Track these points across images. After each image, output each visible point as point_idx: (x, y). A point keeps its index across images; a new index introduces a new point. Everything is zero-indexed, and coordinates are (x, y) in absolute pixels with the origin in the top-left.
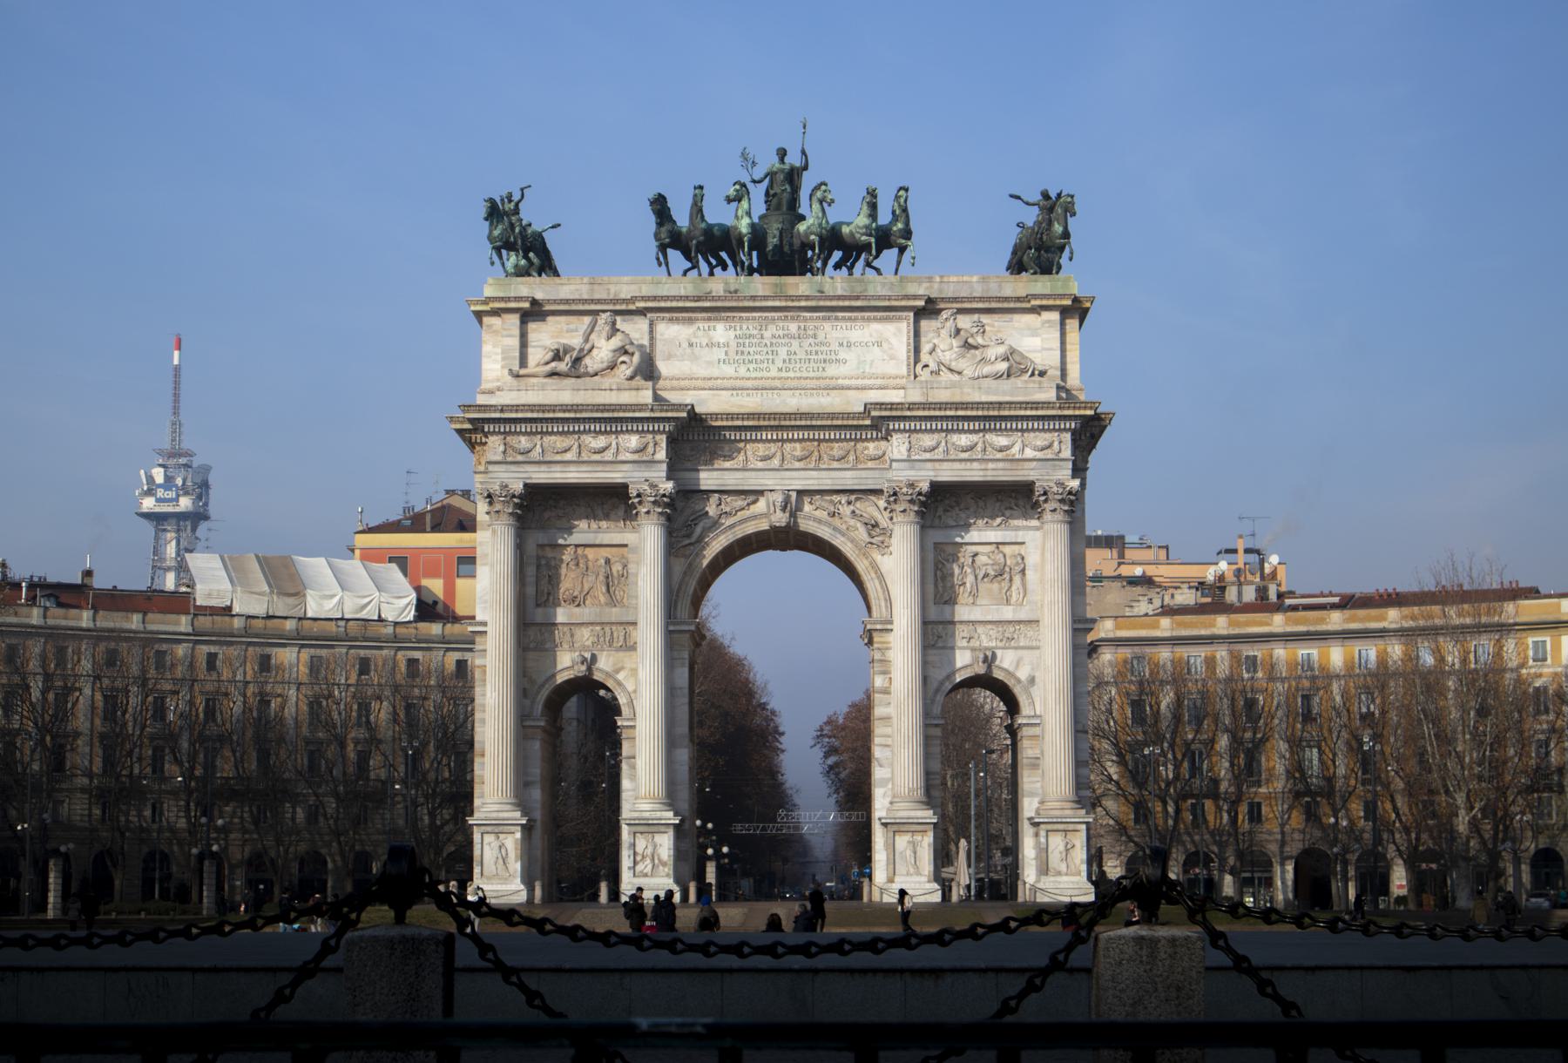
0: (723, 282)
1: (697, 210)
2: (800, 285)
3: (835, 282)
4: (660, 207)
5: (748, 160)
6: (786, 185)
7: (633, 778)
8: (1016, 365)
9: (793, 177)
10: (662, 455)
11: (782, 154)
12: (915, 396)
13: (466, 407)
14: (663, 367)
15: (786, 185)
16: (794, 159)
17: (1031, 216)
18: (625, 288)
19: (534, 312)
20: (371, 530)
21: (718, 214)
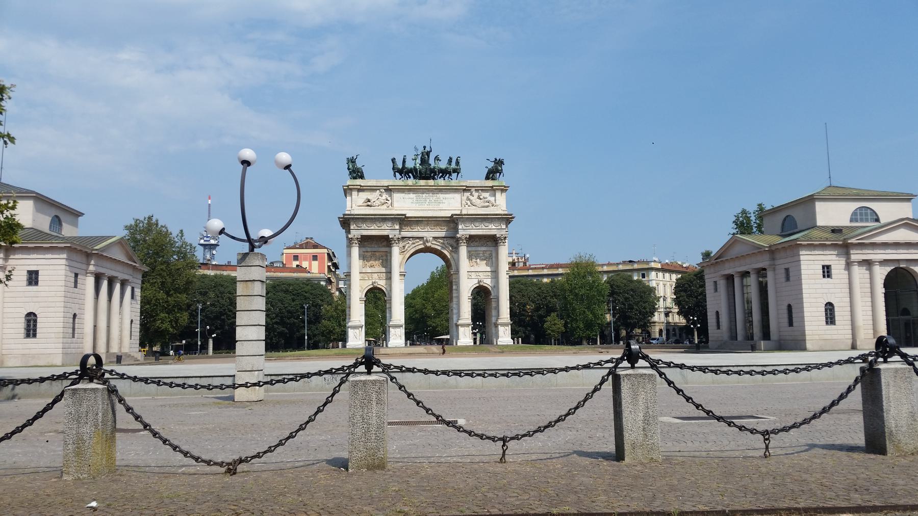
0: (411, 181)
1: (404, 162)
2: (431, 182)
3: (441, 182)
4: (393, 160)
5: (416, 149)
6: (425, 157)
7: (391, 313)
8: (489, 204)
9: (428, 153)
10: (397, 227)
11: (425, 147)
12: (464, 213)
13: (344, 215)
14: (395, 204)
15: (425, 157)
16: (428, 149)
17: (491, 165)
18: (386, 183)
19: (361, 190)
20: (288, 248)
21: (410, 165)
